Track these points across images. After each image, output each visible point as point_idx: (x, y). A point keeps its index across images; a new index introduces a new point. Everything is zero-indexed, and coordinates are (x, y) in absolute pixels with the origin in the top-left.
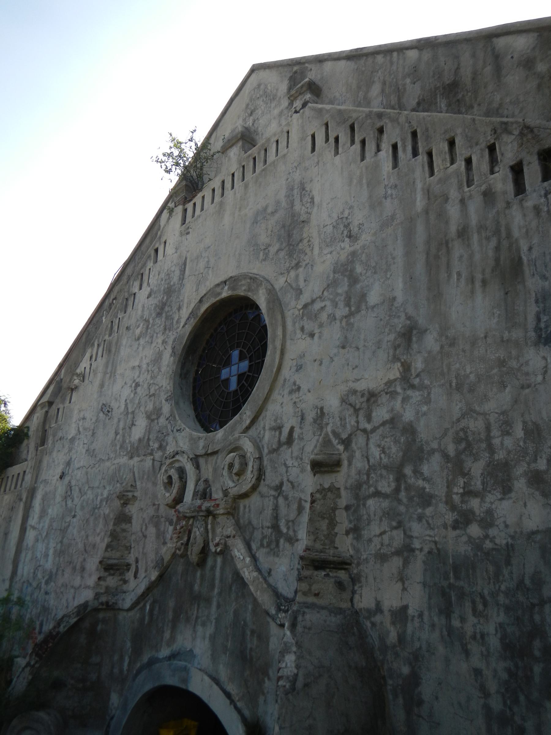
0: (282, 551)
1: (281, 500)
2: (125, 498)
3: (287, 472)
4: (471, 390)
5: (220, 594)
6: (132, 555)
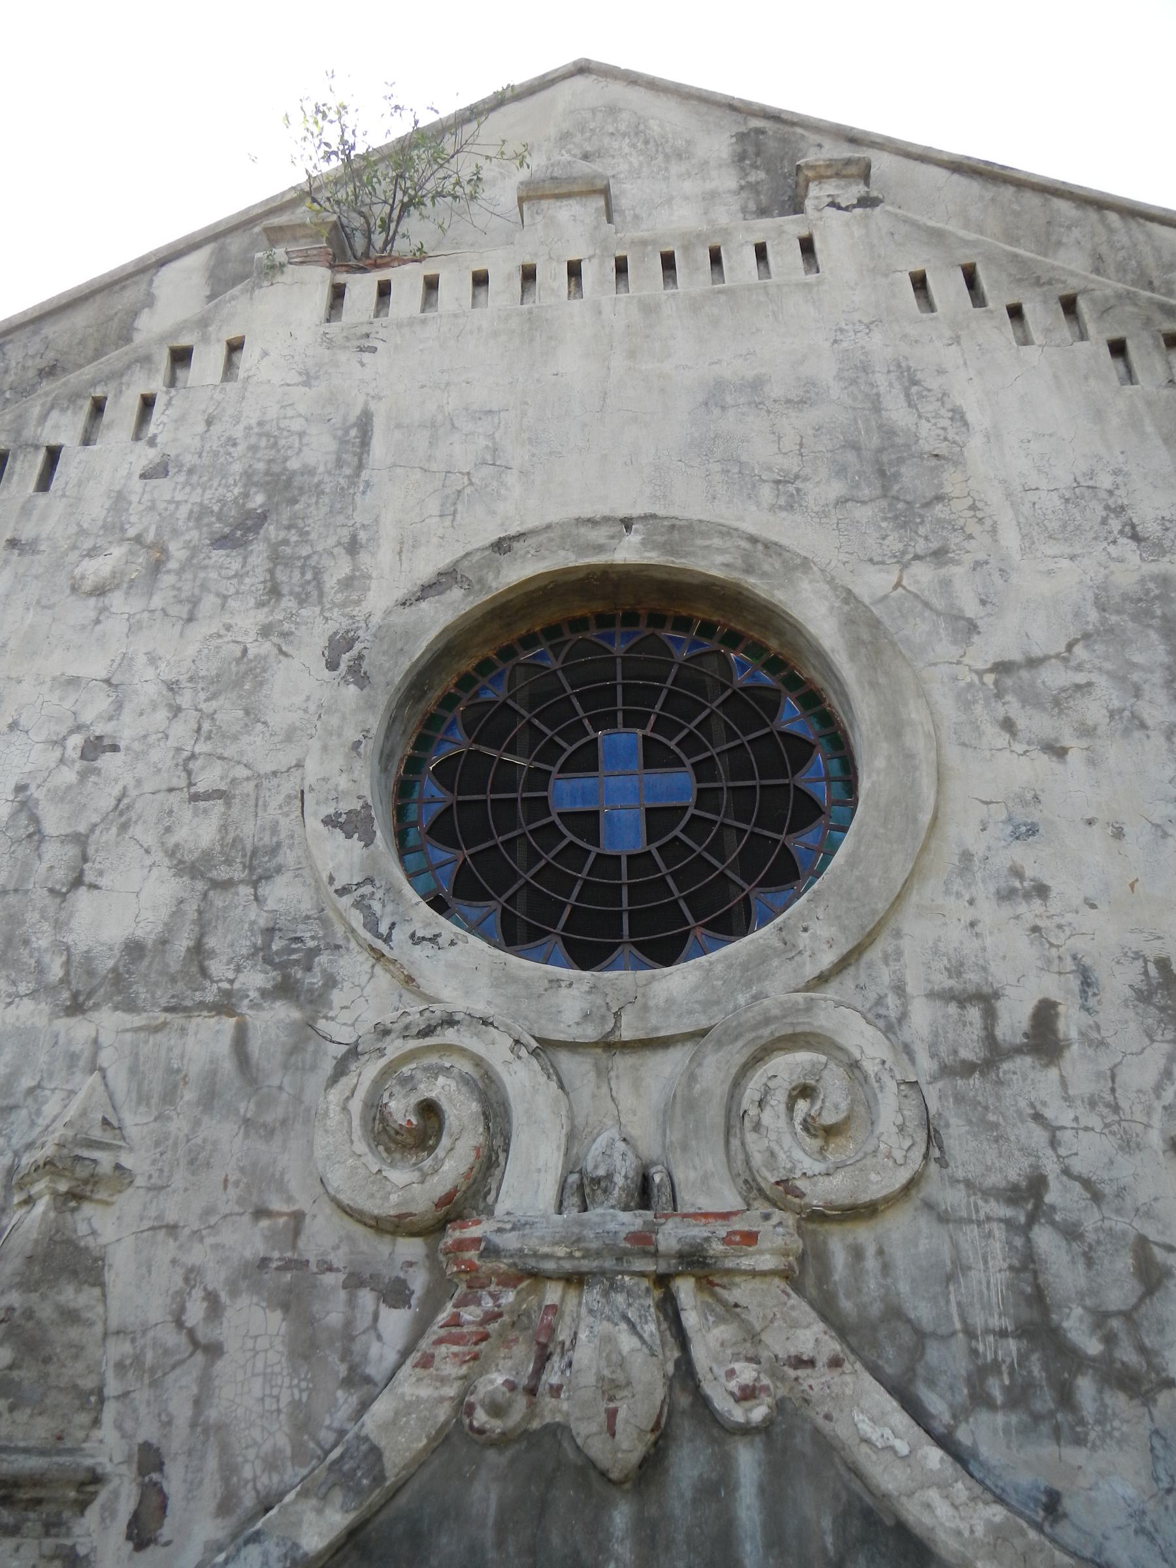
0: (1098, 1422)
2: (82, 1172)
3: (1054, 1143)
6: (108, 1432)
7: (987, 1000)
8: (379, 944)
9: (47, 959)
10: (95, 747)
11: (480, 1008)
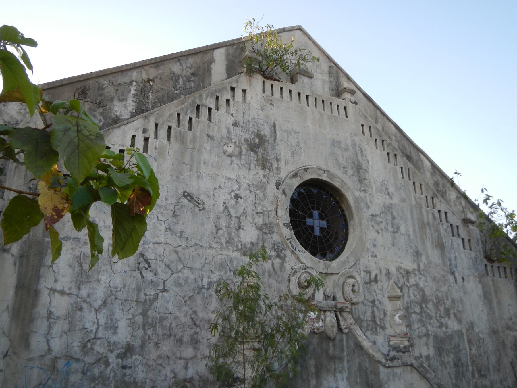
1: (375, 309)
4: (438, 283)
5: (348, 355)
7: (369, 272)
8: (294, 251)
9: (238, 243)
10: (237, 197)
11: (312, 266)
